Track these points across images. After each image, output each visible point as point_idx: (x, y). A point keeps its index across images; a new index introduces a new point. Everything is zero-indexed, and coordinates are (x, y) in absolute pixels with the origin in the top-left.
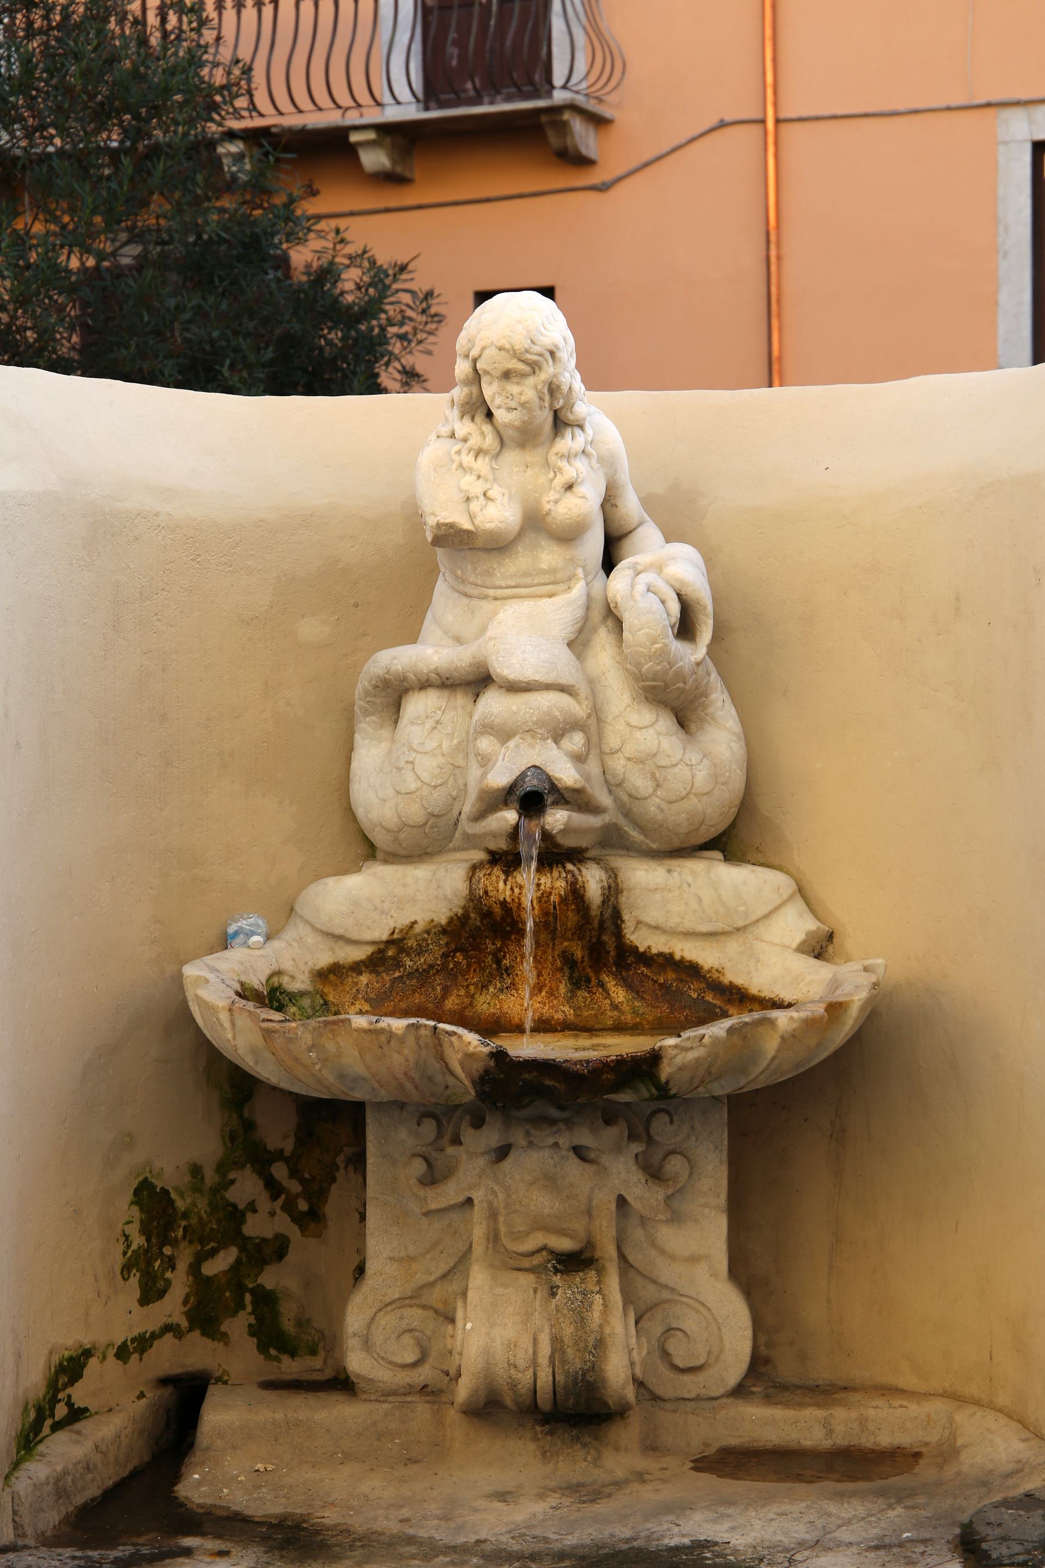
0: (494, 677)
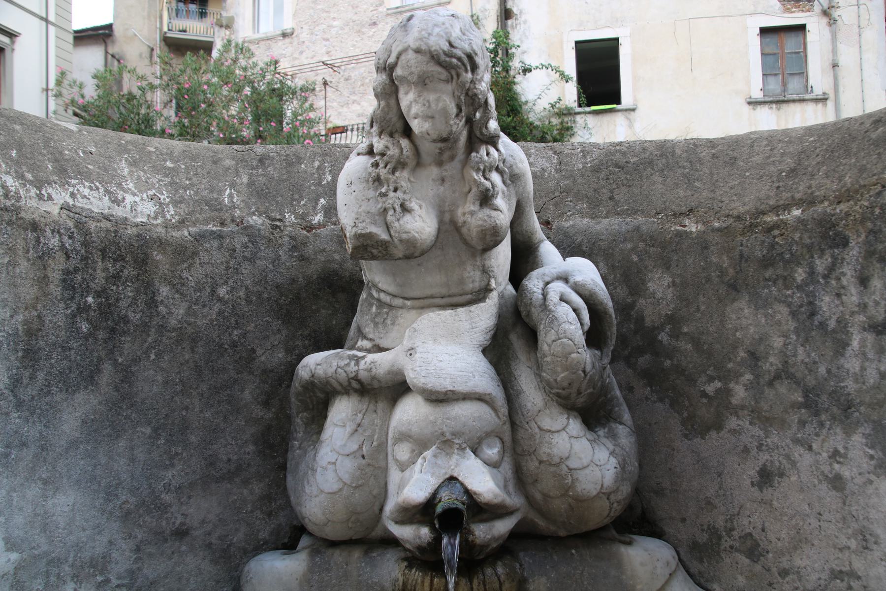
0: (411, 387)
